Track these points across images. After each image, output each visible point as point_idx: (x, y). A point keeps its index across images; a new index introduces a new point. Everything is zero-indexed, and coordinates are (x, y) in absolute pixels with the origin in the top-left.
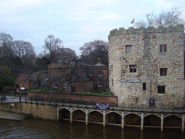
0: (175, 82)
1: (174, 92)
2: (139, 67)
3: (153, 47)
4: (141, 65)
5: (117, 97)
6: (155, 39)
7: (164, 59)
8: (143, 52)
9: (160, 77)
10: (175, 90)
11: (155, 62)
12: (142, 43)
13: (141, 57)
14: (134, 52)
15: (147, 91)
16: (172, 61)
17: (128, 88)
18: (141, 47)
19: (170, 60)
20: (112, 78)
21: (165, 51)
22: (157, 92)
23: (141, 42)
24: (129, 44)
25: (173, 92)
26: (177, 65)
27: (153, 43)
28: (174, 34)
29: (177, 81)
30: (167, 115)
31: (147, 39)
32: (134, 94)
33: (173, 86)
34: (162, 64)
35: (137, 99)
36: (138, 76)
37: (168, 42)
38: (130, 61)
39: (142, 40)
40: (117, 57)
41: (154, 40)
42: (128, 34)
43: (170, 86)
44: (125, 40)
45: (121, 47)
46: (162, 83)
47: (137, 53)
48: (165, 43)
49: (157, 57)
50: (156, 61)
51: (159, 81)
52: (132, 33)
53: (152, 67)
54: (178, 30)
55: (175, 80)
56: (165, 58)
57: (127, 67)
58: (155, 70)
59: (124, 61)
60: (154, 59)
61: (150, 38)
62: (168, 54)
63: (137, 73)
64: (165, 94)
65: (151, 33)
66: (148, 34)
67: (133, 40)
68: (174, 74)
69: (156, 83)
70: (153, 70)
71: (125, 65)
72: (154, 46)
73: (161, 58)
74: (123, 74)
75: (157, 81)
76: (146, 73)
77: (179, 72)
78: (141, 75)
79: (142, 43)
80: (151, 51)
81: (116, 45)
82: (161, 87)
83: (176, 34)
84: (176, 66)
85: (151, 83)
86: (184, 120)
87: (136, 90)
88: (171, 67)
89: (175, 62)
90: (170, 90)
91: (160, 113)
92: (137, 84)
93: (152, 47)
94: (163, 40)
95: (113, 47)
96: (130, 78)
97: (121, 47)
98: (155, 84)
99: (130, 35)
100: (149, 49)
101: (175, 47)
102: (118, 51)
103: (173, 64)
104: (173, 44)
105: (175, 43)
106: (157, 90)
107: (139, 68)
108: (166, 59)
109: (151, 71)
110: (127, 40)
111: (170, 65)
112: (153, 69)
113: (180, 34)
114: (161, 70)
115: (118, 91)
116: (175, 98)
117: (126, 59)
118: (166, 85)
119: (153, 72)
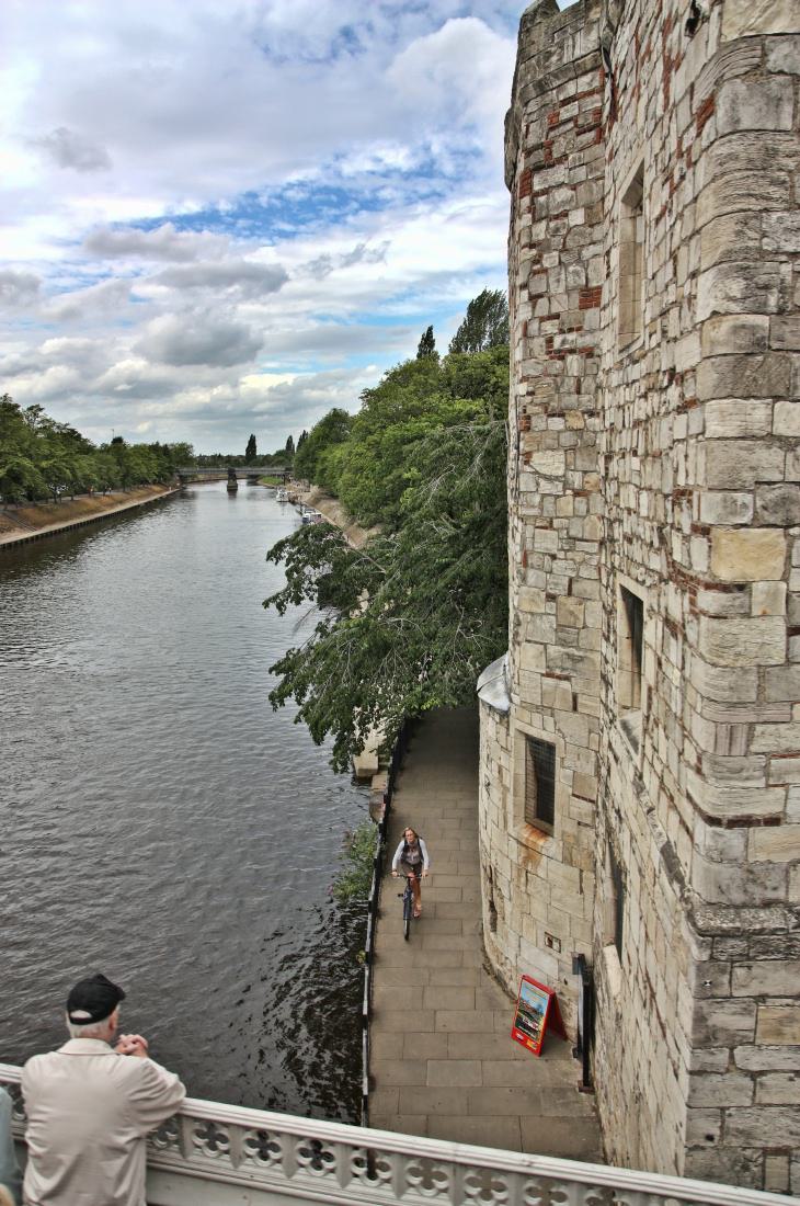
31: (559, 174)
66: (584, 83)
76: (547, 624)
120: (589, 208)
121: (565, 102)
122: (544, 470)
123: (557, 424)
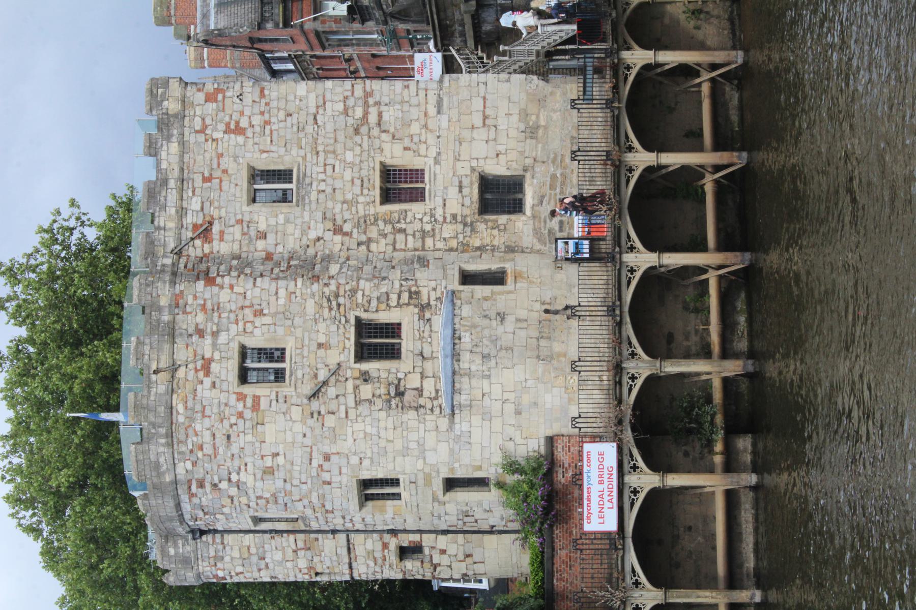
0: (459, 121)
1: (509, 124)
2: (369, 302)
3: (263, 236)
4: (360, 293)
5: (550, 441)
6: (216, 229)
7: (330, 181)
8: (282, 283)
9: (433, 202)
10: (502, 124)
11: (347, 228)
12: (232, 287)
13: (313, 295)
14: (280, 331)
15: (508, 266)
16: (341, 137)
17: (493, 362)
18: (257, 290)
19: (339, 148)
20: (438, 485)
21: (284, 175)
22: (513, 217)
23: (225, 296)
24: (233, 366)
25: (513, 133)
26: (366, 114)
27: (238, 236)
28: (198, 128)
29: (454, 113)
30: (627, 137)
32: (524, 325)
33: (481, 134)
34: (357, 190)
35: (556, 312)
36: (424, 308)
37: (236, 157)
38: (334, 357)
39: (215, 289)
40: (308, 441)
41: (222, 233)
42: (174, 368)
43: (480, 149)
44: (205, 391)
45: (248, 414)
46: (466, 191)
47: (286, 314)
48: (244, 175)
49: (319, 215)
50: (339, 222)
51: (454, 207)
52: (167, 347)
53: (373, 246)
54: (172, 106)
55: (445, 124)
56: (322, 176)
57: (365, 377)
58: (389, 229)
59: (331, 391)
60: (328, 235)
61: (205, 255)
62: (304, 158)
63: (406, 317)
64: (528, 175)
65: (179, 253)
67: (208, 340)
68: (415, 128)
69: (465, 225)
70: (390, 238)
71: (356, 387)
72: (253, 233)
73: (322, 196)
74: (408, 397)
75: (454, 216)
76: (405, 268)
77: (402, 102)
78: (414, 295)
79: (232, 287)
80: (280, 249)
81: (235, 449)
82: (489, 196)
83: (198, 120)
84: (373, 118)
85: (465, 248)
86: (651, 53)
87: (502, 317)
88: (377, 142)
89: (350, 121)
90: (502, 148)
91: (618, 169)
92: (466, 311)
93: (260, 244)
94: (225, 185)
95: (243, 477)
96: (432, 358)
97: (248, 414)
98: (468, 229)
99: (182, 355)
100: (269, 257)
101: (267, 123)
102: (270, 431)
103: (357, 131)
104: (249, 133)
105: (244, 123)
106: (503, 219)
107: (374, 303)
108: (329, 168)
109: (395, 249)
110: (207, 374)
111: (365, 146)
112: (385, 236)
113: (200, 97)
114: (387, 196)
115: (510, 431)
116: (542, 123)
117: (321, 377)
118: (473, 170)
119: (400, 237)
120: (233, 259)
121: (186, 266)
122: (337, 271)
123: (318, 267)
